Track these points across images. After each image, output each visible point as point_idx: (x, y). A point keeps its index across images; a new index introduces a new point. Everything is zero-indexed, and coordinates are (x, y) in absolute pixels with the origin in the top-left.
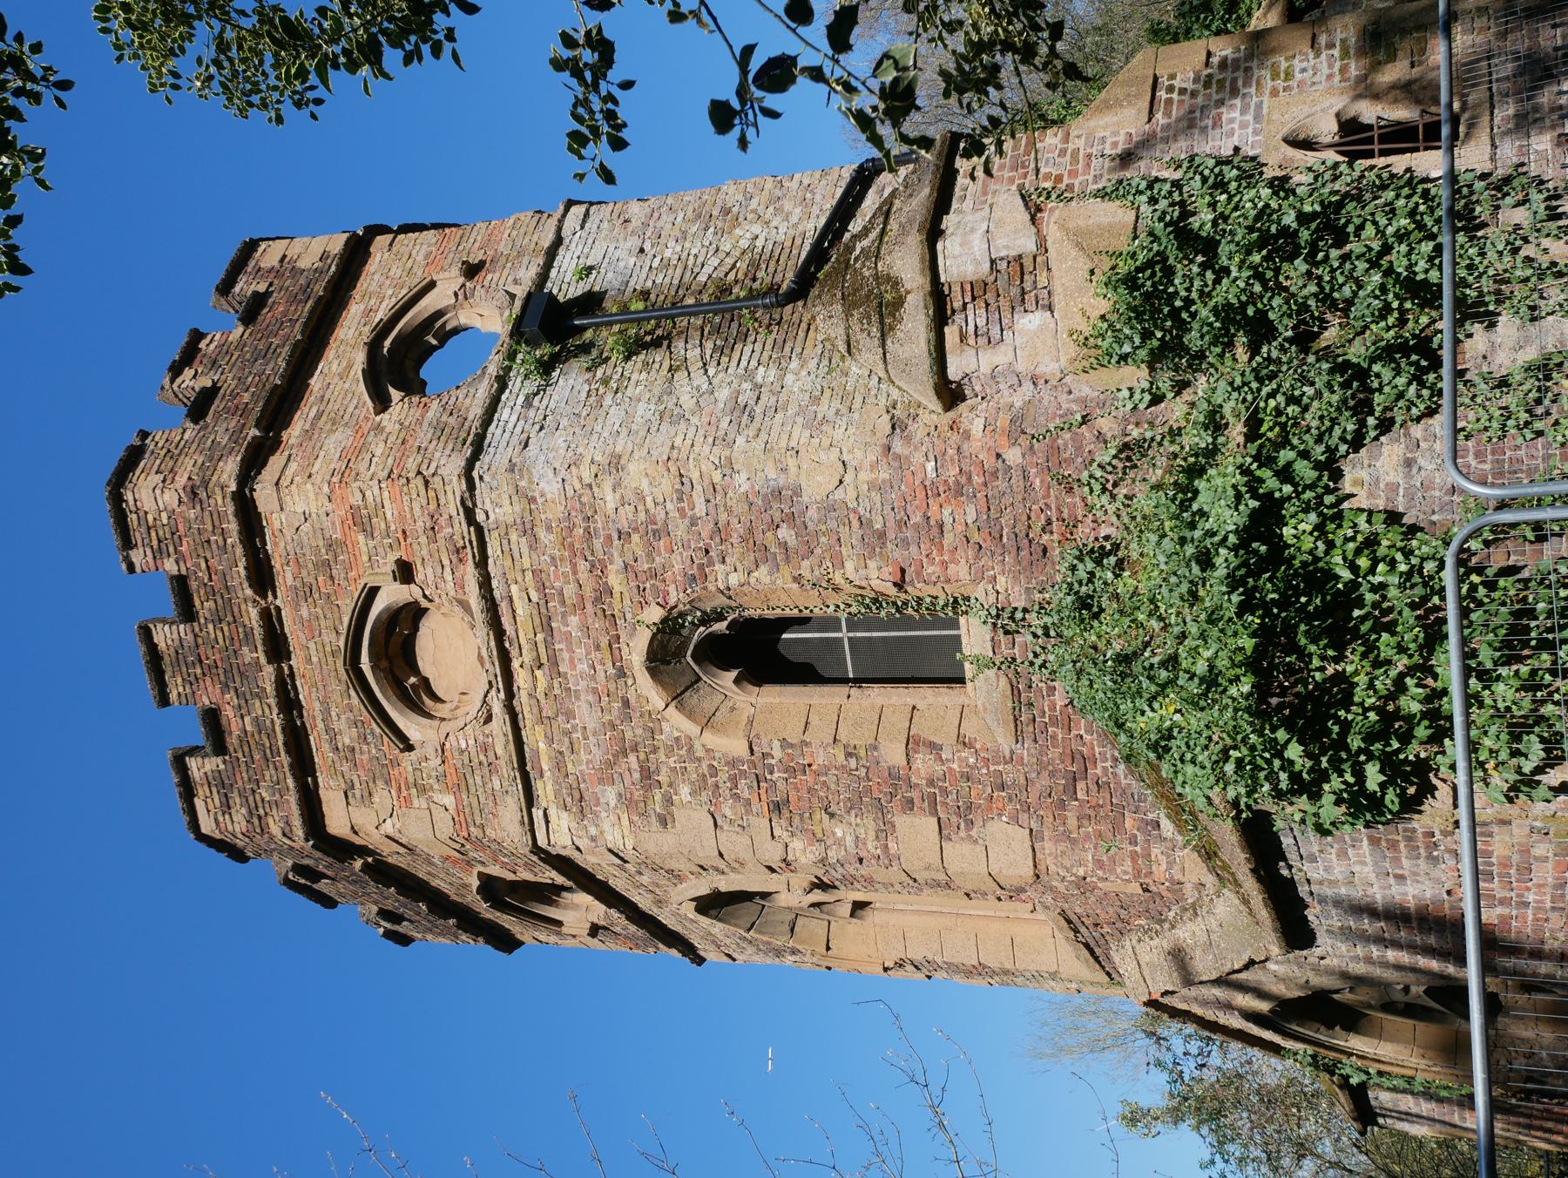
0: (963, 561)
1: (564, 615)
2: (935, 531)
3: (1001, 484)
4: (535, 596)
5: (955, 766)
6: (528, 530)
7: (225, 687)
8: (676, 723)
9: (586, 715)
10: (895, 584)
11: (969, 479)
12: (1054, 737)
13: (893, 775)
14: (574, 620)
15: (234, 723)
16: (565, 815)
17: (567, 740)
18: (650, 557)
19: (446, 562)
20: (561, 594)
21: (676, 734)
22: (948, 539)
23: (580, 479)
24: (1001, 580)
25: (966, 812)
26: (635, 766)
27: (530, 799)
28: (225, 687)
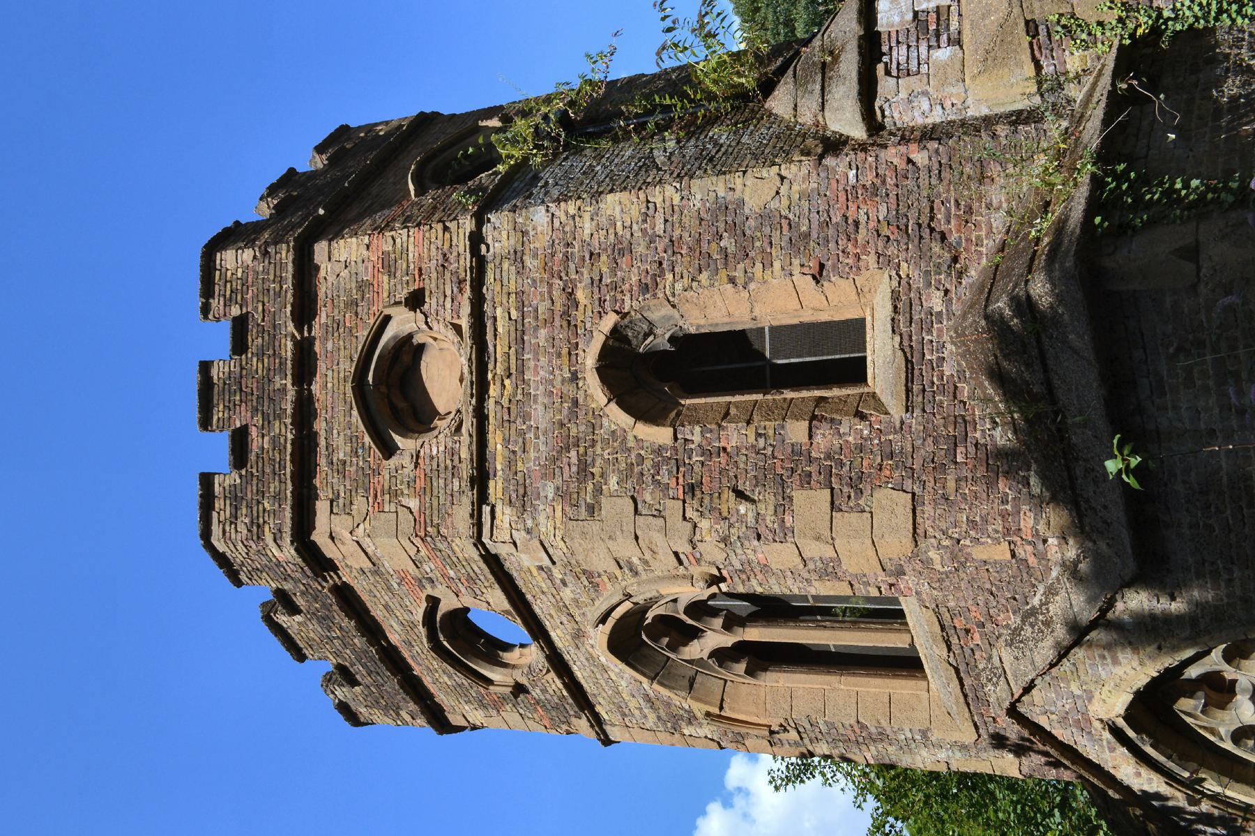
0: (873, 252)
1: (537, 328)
2: (851, 228)
3: (910, 183)
4: (514, 314)
5: (851, 439)
6: (517, 257)
8: (618, 417)
9: (540, 415)
10: (814, 277)
11: (884, 182)
12: (941, 402)
13: (796, 451)
14: (543, 333)
15: (257, 441)
16: (508, 510)
17: (521, 440)
18: (613, 272)
19: (448, 292)
20: (536, 310)
21: (613, 427)
22: (861, 237)
23: (567, 213)
24: (904, 265)
25: (856, 483)
26: (574, 460)
27: (483, 498)
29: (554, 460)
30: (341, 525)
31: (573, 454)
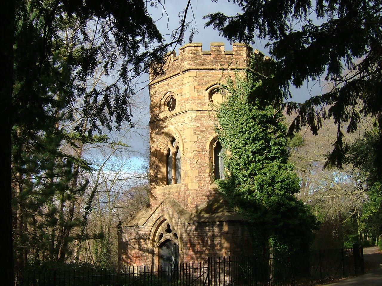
5: (206, 179)
7: (214, 58)
28: (214, 58)
29: (204, 125)
30: (191, 79)
31: (205, 129)
